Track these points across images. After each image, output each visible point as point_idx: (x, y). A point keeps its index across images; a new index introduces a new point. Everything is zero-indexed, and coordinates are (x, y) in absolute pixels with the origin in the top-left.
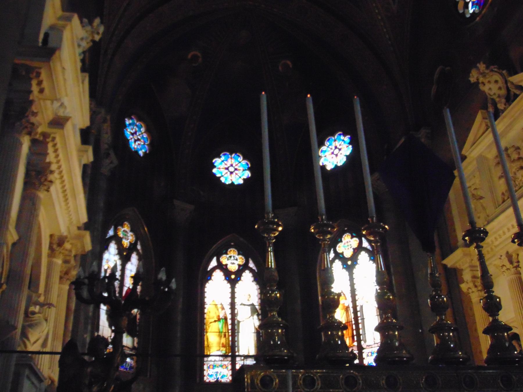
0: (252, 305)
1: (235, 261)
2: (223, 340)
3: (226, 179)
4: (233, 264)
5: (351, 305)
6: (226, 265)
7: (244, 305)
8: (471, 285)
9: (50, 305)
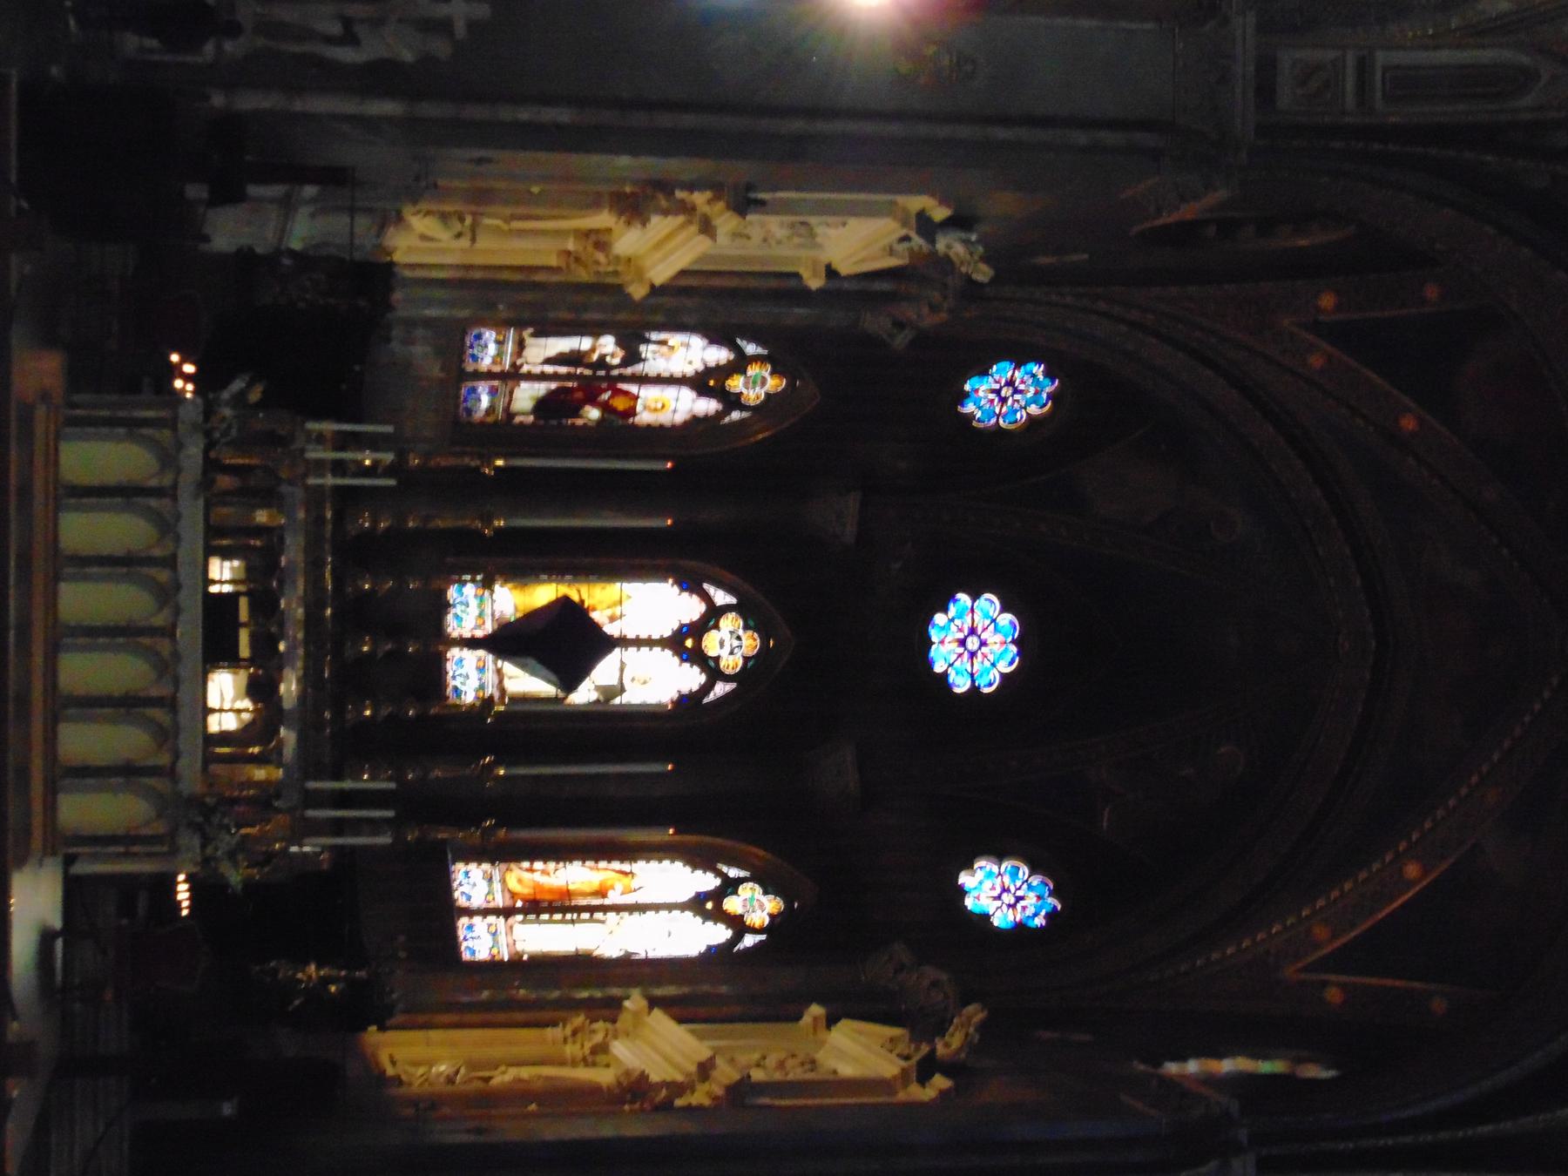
0: (622, 690)
1: (727, 649)
3: (942, 628)
4: (722, 644)
5: (607, 902)
6: (716, 627)
7: (622, 670)
9: (473, 240)
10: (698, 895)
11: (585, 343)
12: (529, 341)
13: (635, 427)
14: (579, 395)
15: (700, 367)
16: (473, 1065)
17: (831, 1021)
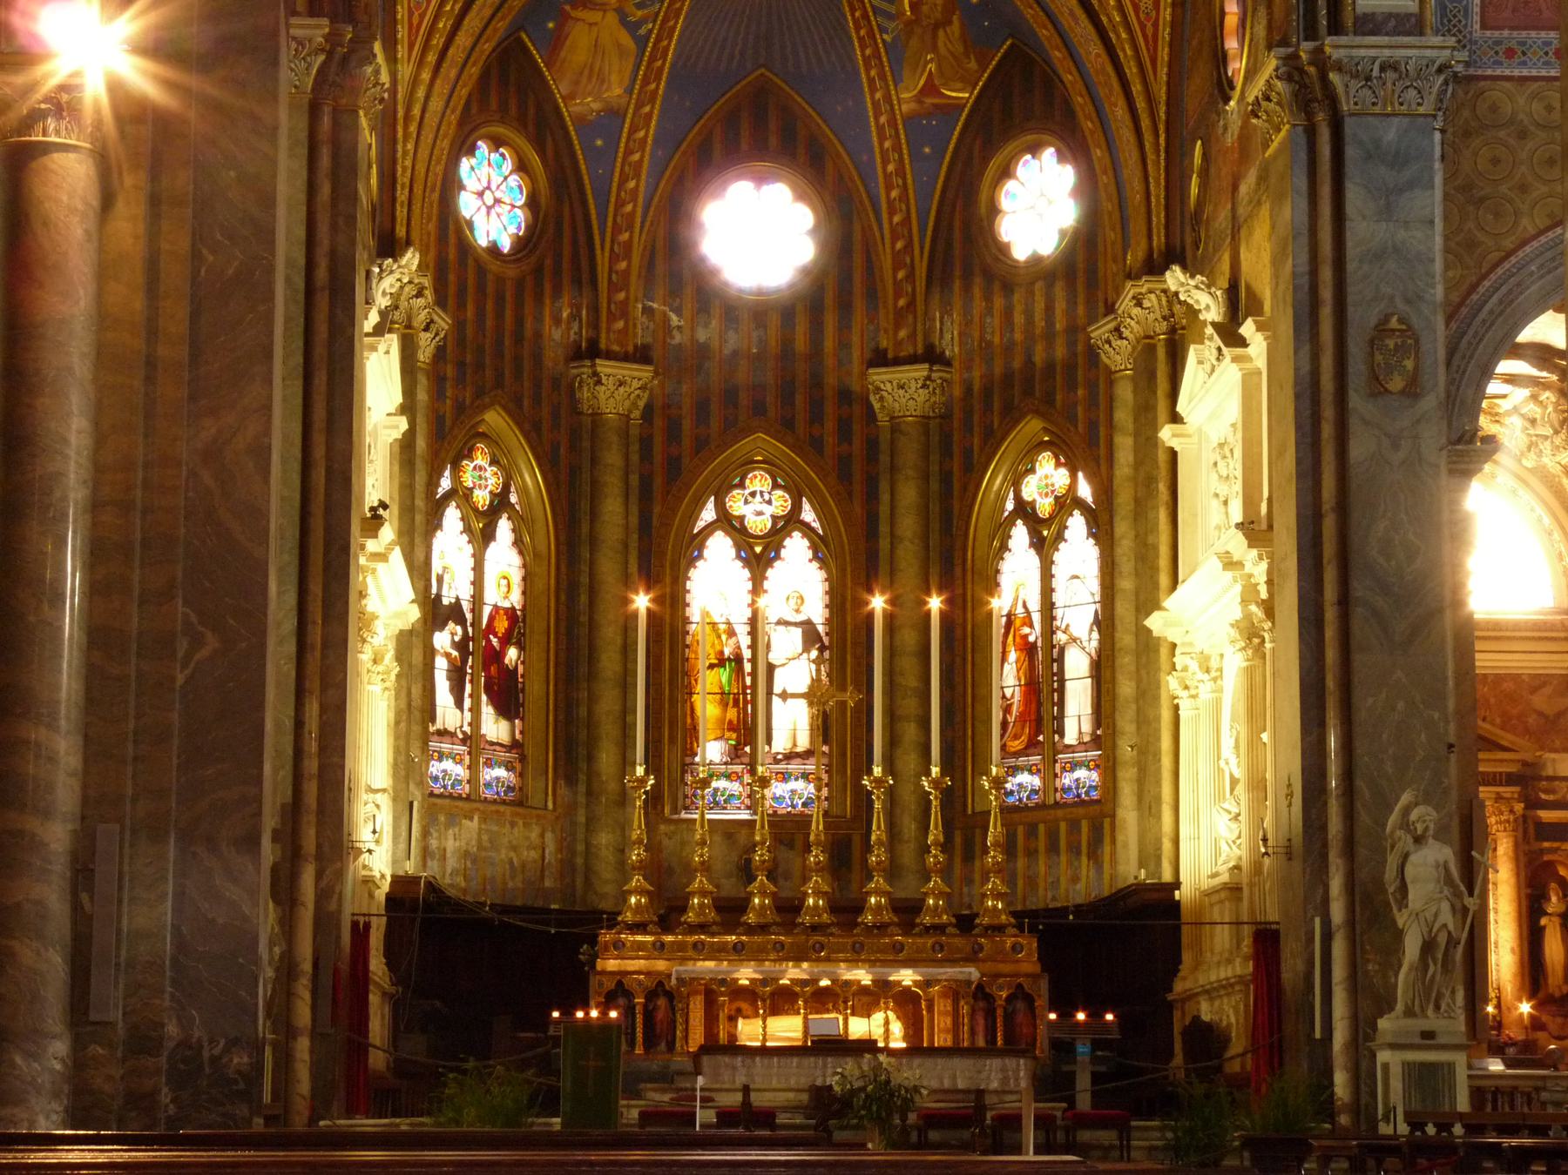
0: (808, 627)
2: (732, 714)
4: (760, 513)
7: (787, 623)
10: (1032, 545)
11: (441, 664)
12: (439, 725)
13: (524, 609)
15: (465, 538)
16: (1219, 797)
17: (1175, 418)
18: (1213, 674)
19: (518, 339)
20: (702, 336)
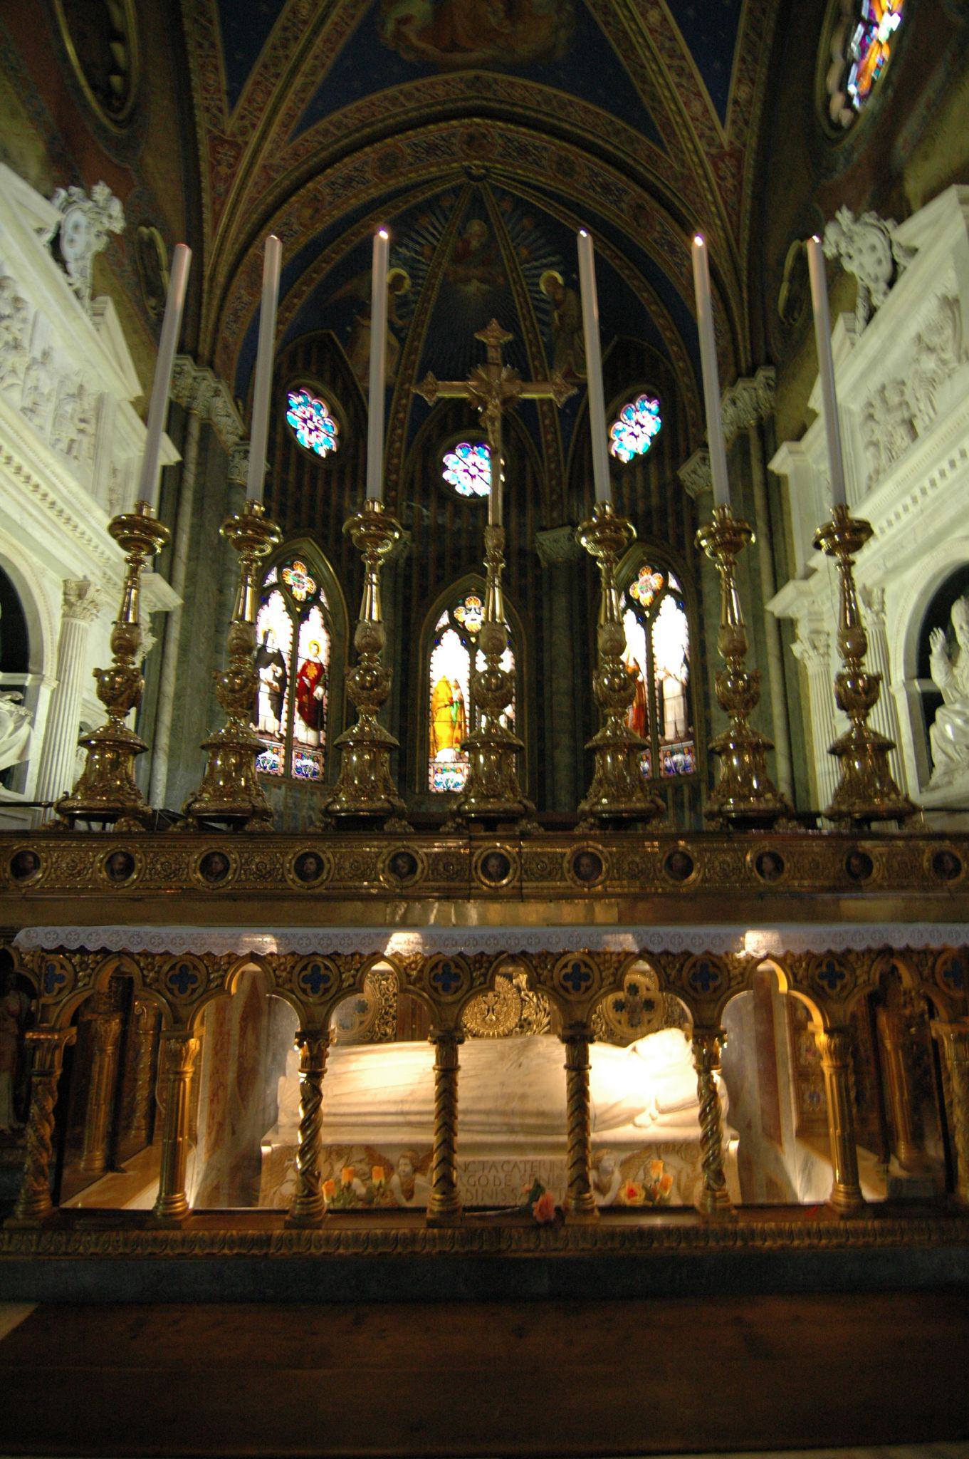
2: (458, 733)
8: (807, 646)
12: (261, 727)
14: (305, 698)
15: (286, 615)
18: (876, 607)
19: (326, 501)
20: (440, 521)
